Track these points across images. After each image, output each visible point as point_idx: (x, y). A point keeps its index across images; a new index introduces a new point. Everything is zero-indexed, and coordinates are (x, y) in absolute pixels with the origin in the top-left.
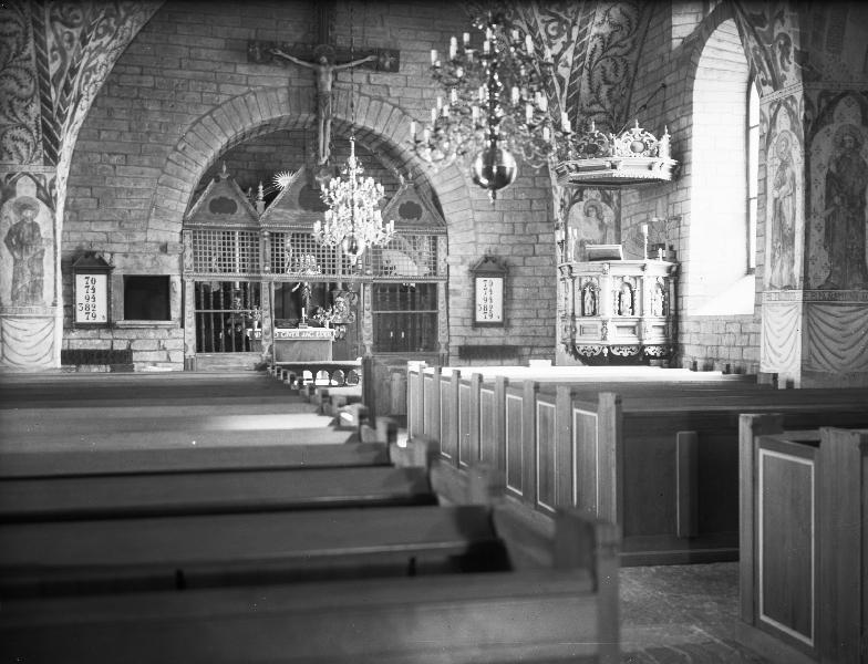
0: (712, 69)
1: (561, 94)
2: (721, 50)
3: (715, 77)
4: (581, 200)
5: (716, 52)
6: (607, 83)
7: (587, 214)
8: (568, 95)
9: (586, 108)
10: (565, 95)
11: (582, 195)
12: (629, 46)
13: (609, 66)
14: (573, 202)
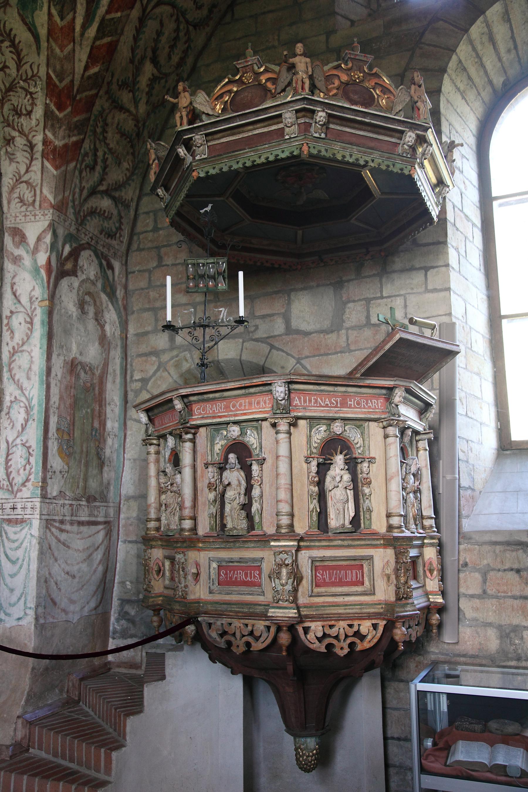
0: (465, 69)
1: (85, 27)
2: (492, 40)
3: (462, 87)
4: (73, 273)
5: (485, 38)
6: (155, 61)
7: (82, 305)
8: (96, 38)
9: (114, 87)
10: (92, 32)
11: (76, 260)
12: (205, 12)
13: (170, 26)
14: (62, 274)
